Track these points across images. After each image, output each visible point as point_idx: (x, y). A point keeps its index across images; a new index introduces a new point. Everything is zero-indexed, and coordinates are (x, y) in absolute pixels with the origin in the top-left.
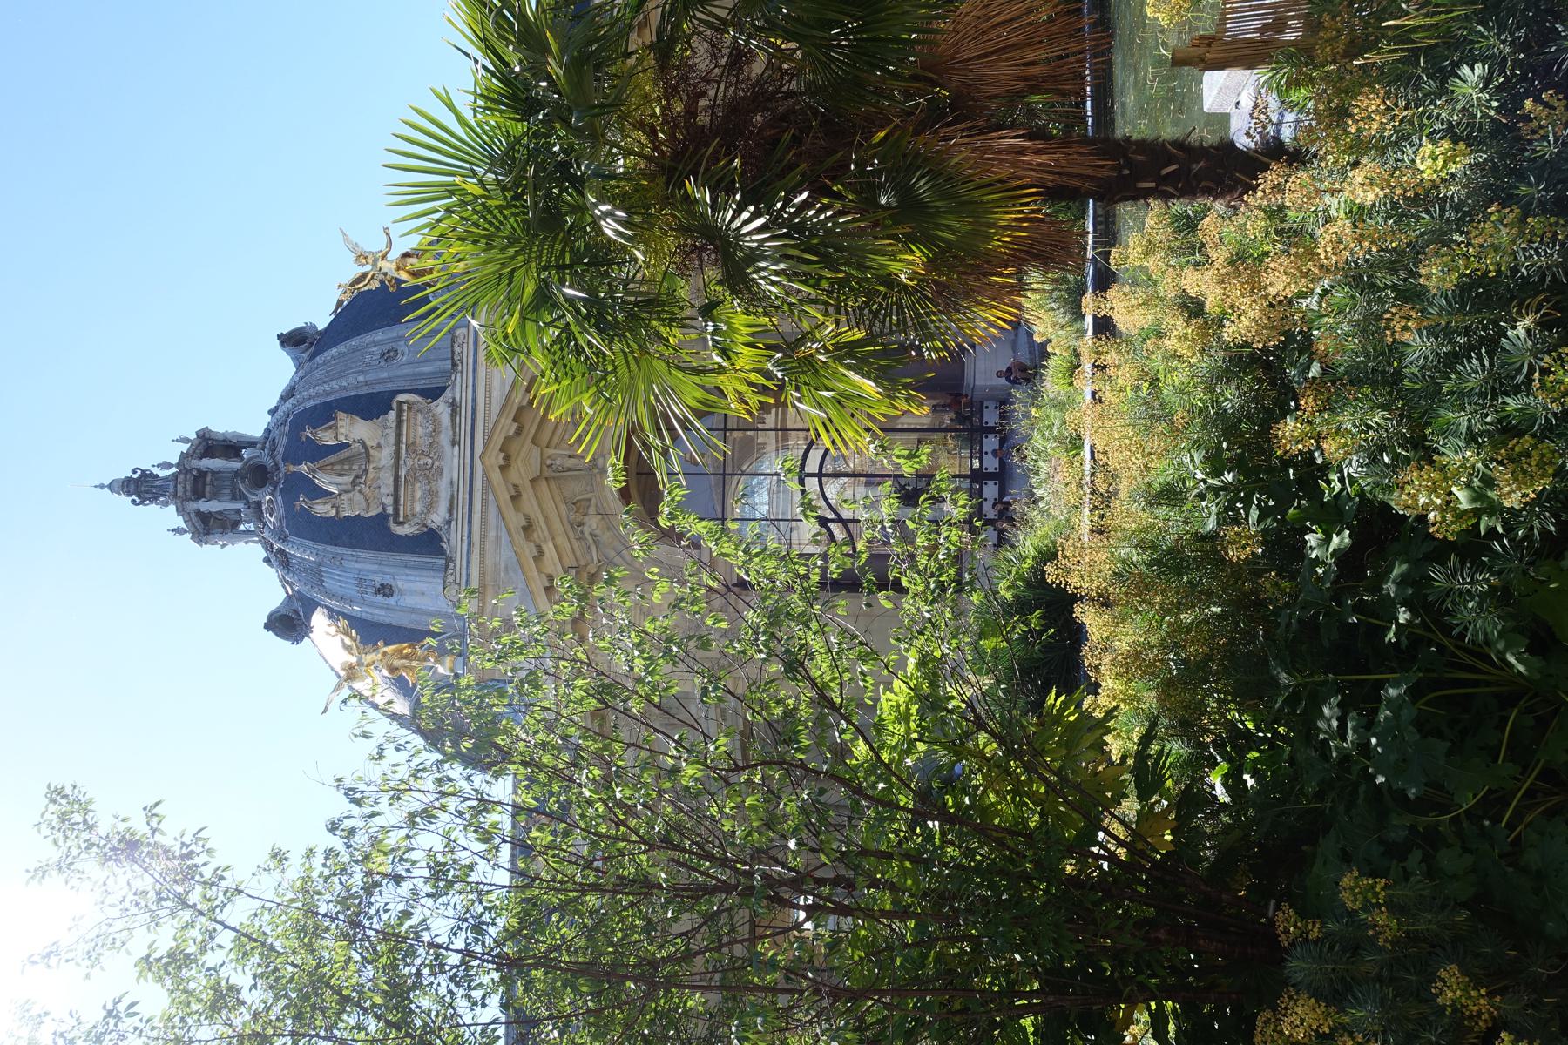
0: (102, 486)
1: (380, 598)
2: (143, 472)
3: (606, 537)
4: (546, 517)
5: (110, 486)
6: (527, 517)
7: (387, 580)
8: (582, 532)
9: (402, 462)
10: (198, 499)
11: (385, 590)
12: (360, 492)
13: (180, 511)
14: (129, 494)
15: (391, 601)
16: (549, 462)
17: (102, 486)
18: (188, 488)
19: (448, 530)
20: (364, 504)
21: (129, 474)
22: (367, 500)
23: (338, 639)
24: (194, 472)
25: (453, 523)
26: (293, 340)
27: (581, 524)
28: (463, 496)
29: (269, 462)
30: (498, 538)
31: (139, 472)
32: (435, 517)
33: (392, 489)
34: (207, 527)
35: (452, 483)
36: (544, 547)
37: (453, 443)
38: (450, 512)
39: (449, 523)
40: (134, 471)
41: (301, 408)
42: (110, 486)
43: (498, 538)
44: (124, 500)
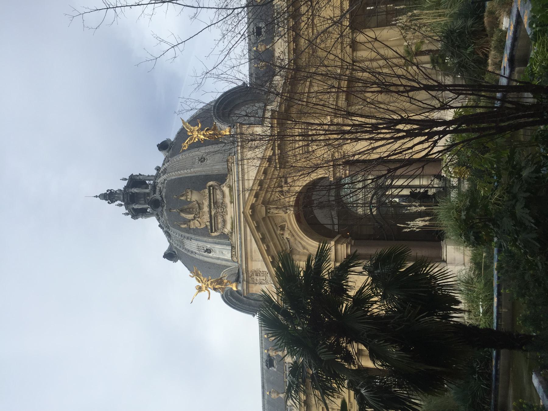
0: (96, 196)
1: (206, 254)
2: (111, 190)
3: (292, 240)
4: (269, 232)
5: (99, 196)
6: (262, 234)
7: (209, 246)
8: (283, 237)
9: (212, 210)
10: (132, 203)
11: (208, 251)
12: (197, 220)
13: (126, 209)
14: (106, 200)
15: (211, 255)
16: (269, 211)
17: (96, 196)
18: (129, 199)
19: (232, 236)
20: (199, 224)
21: (106, 192)
22: (200, 223)
23: (194, 278)
24: (130, 194)
25: (234, 233)
26: (163, 146)
27: (283, 234)
28: (237, 223)
29: (160, 198)
30: (251, 240)
31: (109, 191)
32: (226, 230)
33: (209, 220)
34: (136, 214)
35: (231, 218)
36: (269, 244)
37: (232, 202)
38: (232, 229)
39: (231, 233)
40: (108, 191)
41: (170, 178)
42: (99, 196)
43: (251, 240)
44: (105, 202)
